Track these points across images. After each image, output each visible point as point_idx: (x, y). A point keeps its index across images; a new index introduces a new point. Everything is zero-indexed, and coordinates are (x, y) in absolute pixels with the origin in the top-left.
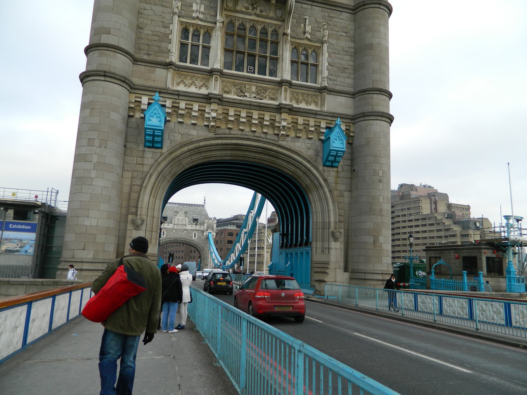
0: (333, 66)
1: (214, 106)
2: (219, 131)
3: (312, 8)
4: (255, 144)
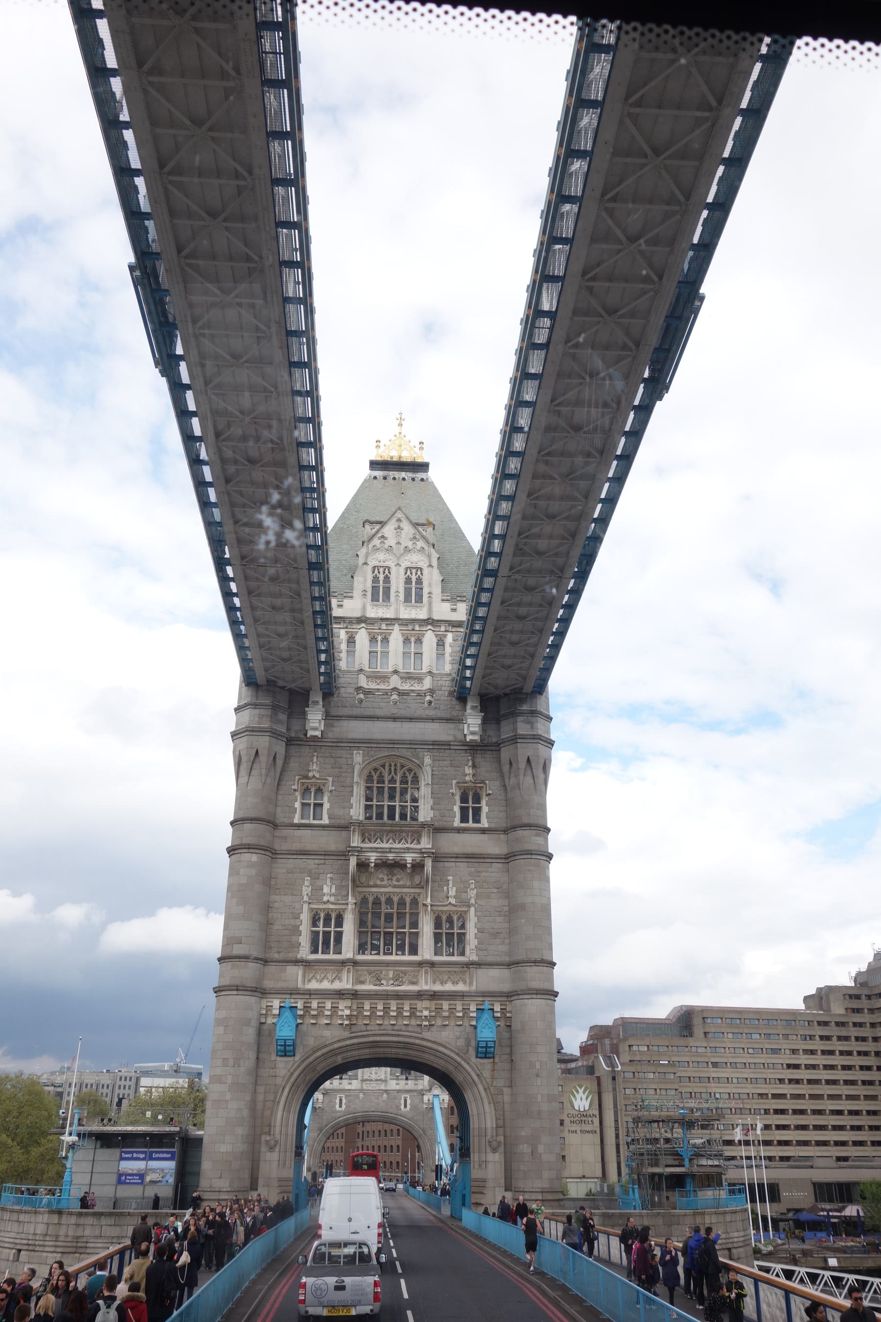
2: (354, 1029)
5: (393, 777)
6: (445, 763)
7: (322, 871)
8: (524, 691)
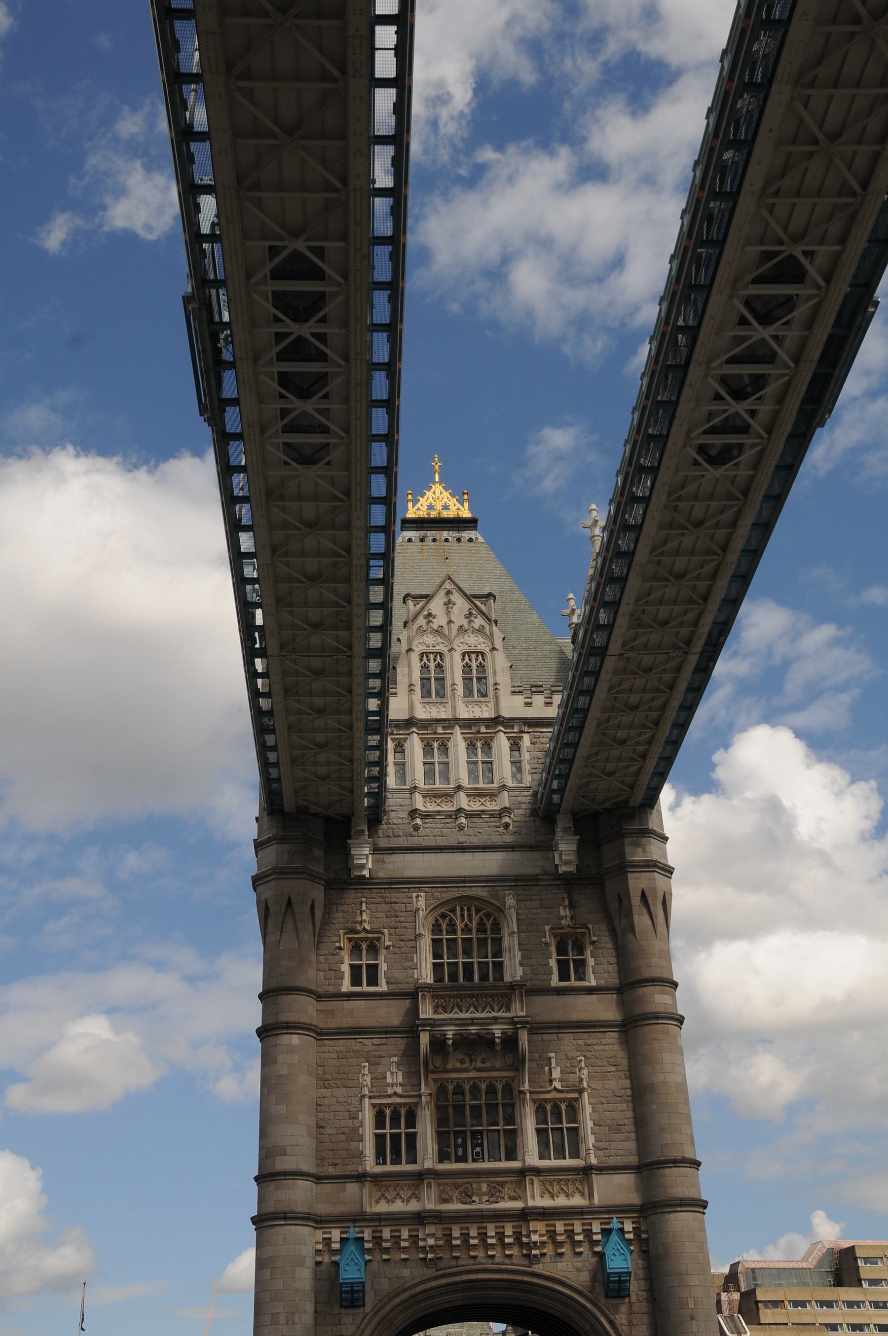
0: (600, 1126)
1: (430, 1229)
2: (441, 1264)
3: (558, 1037)
5: (466, 925)
6: (536, 903)
7: (384, 1054)
8: (631, 804)
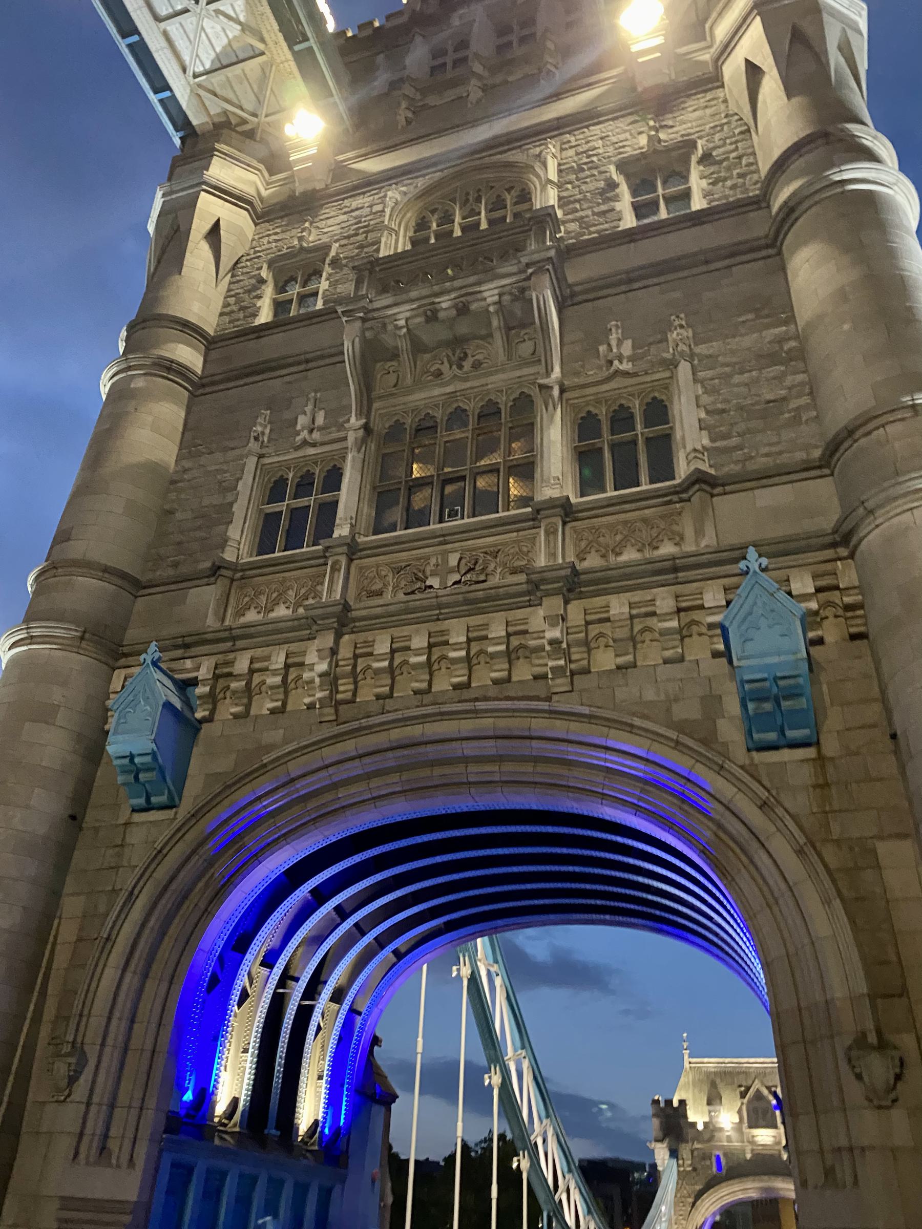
4: (467, 726)
